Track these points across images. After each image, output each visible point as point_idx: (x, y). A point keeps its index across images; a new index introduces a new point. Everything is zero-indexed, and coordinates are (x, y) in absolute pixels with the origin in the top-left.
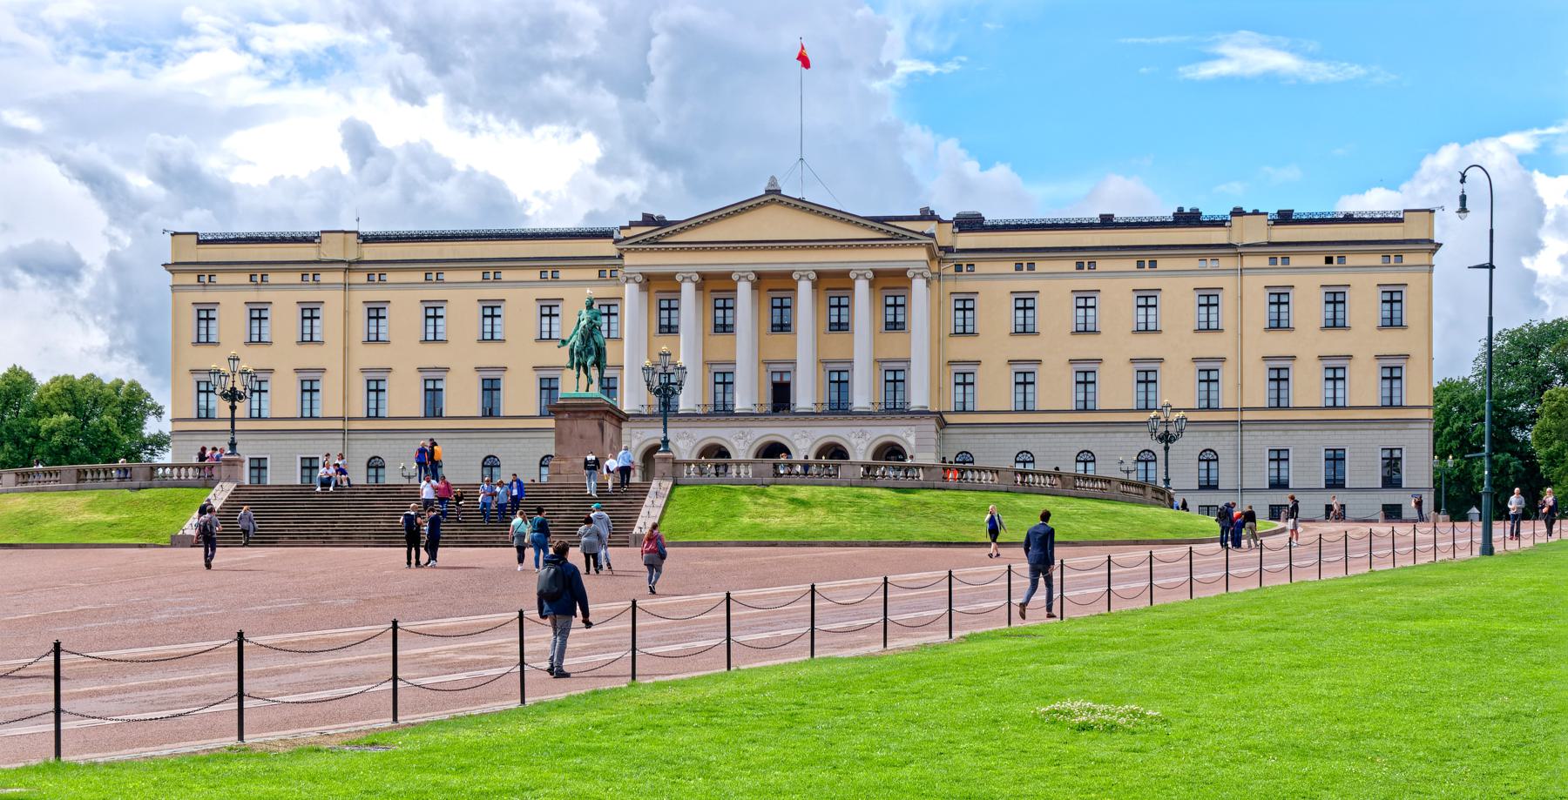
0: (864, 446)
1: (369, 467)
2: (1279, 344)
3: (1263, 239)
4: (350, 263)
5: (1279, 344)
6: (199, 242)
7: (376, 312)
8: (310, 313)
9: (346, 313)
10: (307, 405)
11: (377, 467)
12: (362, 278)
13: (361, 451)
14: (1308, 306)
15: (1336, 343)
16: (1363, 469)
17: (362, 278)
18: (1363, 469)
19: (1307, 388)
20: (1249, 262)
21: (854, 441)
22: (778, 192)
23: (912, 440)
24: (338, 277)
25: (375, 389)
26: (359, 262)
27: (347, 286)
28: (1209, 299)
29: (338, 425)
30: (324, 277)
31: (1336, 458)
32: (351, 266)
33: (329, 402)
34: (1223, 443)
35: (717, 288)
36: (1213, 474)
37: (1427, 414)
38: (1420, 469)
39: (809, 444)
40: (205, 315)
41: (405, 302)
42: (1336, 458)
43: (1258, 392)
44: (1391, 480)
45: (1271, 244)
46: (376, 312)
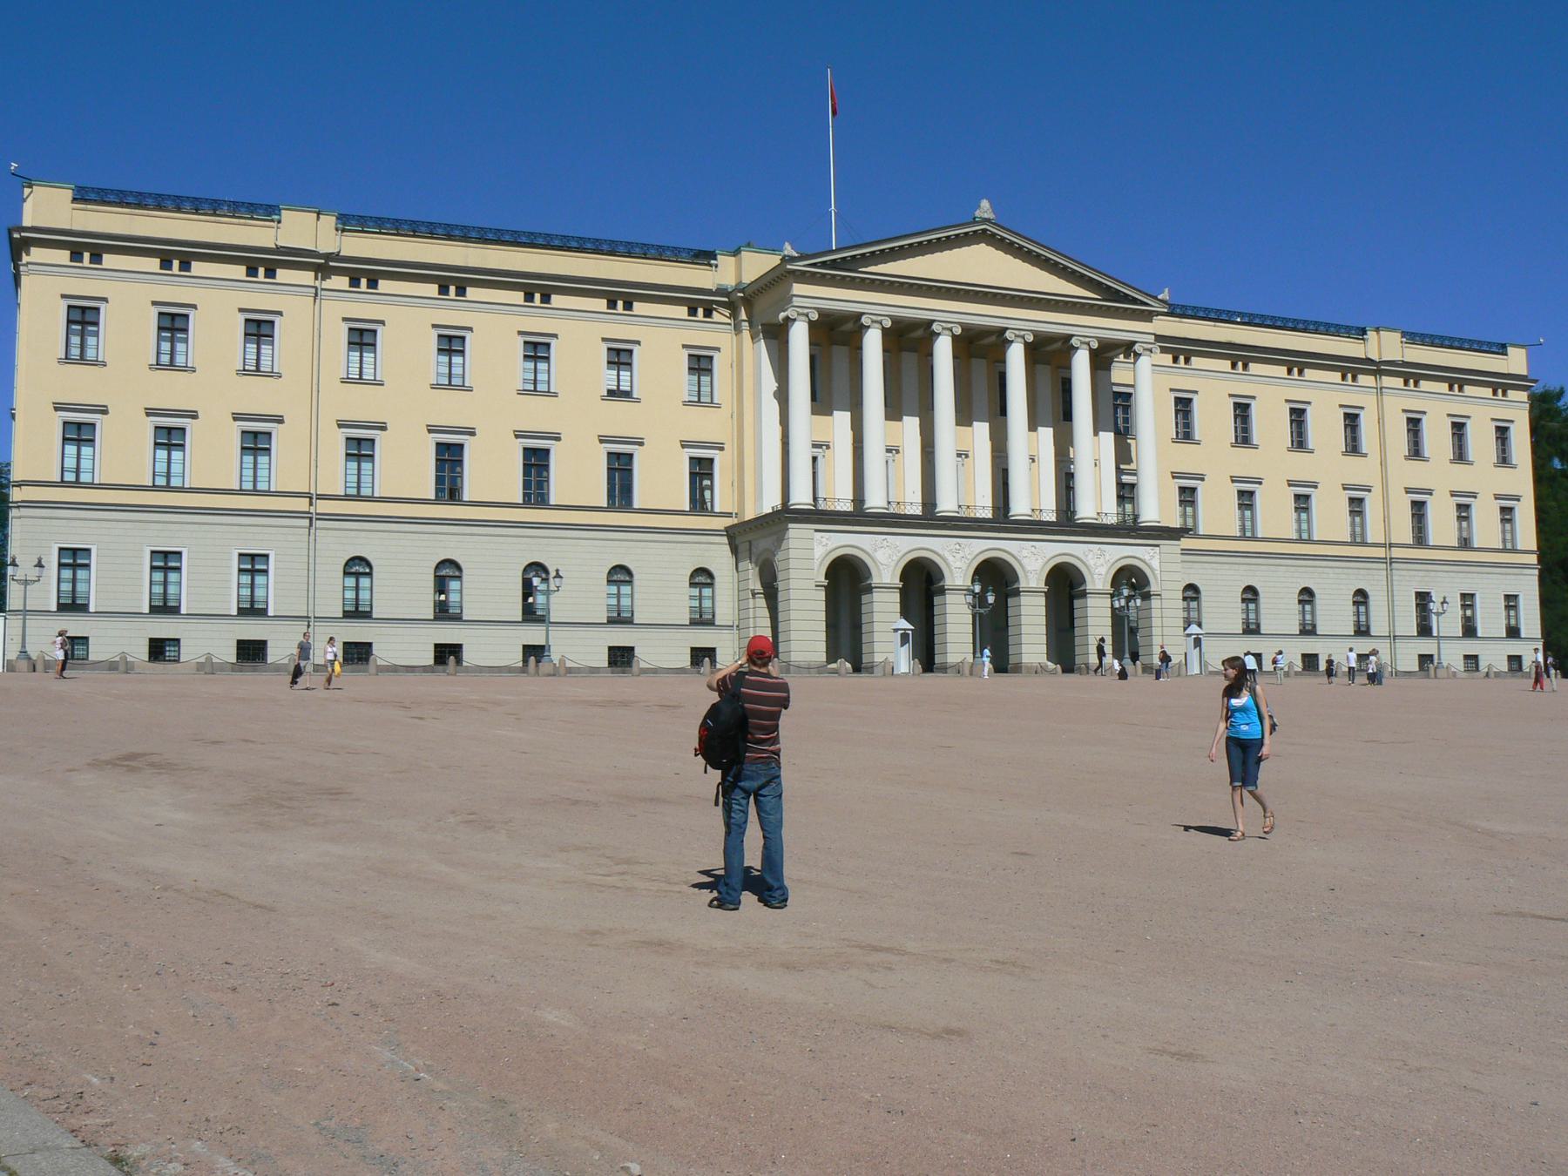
0: (1103, 570)
1: (346, 574)
2: (1417, 474)
3: (1398, 358)
4: (329, 257)
5: (1417, 474)
6: (75, 200)
7: (362, 338)
8: (259, 329)
9: (317, 335)
10: (249, 473)
12: (341, 282)
13: (339, 545)
14: (1437, 437)
15: (1462, 477)
16: (1491, 620)
17: (341, 282)
19: (1441, 525)
20: (1387, 381)
21: (1091, 562)
24: (307, 277)
25: (360, 450)
26: (336, 257)
28: (1352, 420)
29: (302, 505)
30: (283, 275)
32: (324, 265)
33: (287, 466)
34: (1374, 583)
35: (909, 341)
36: (1363, 618)
37: (1533, 559)
39: (1040, 562)
45: (1405, 364)
46: (362, 338)
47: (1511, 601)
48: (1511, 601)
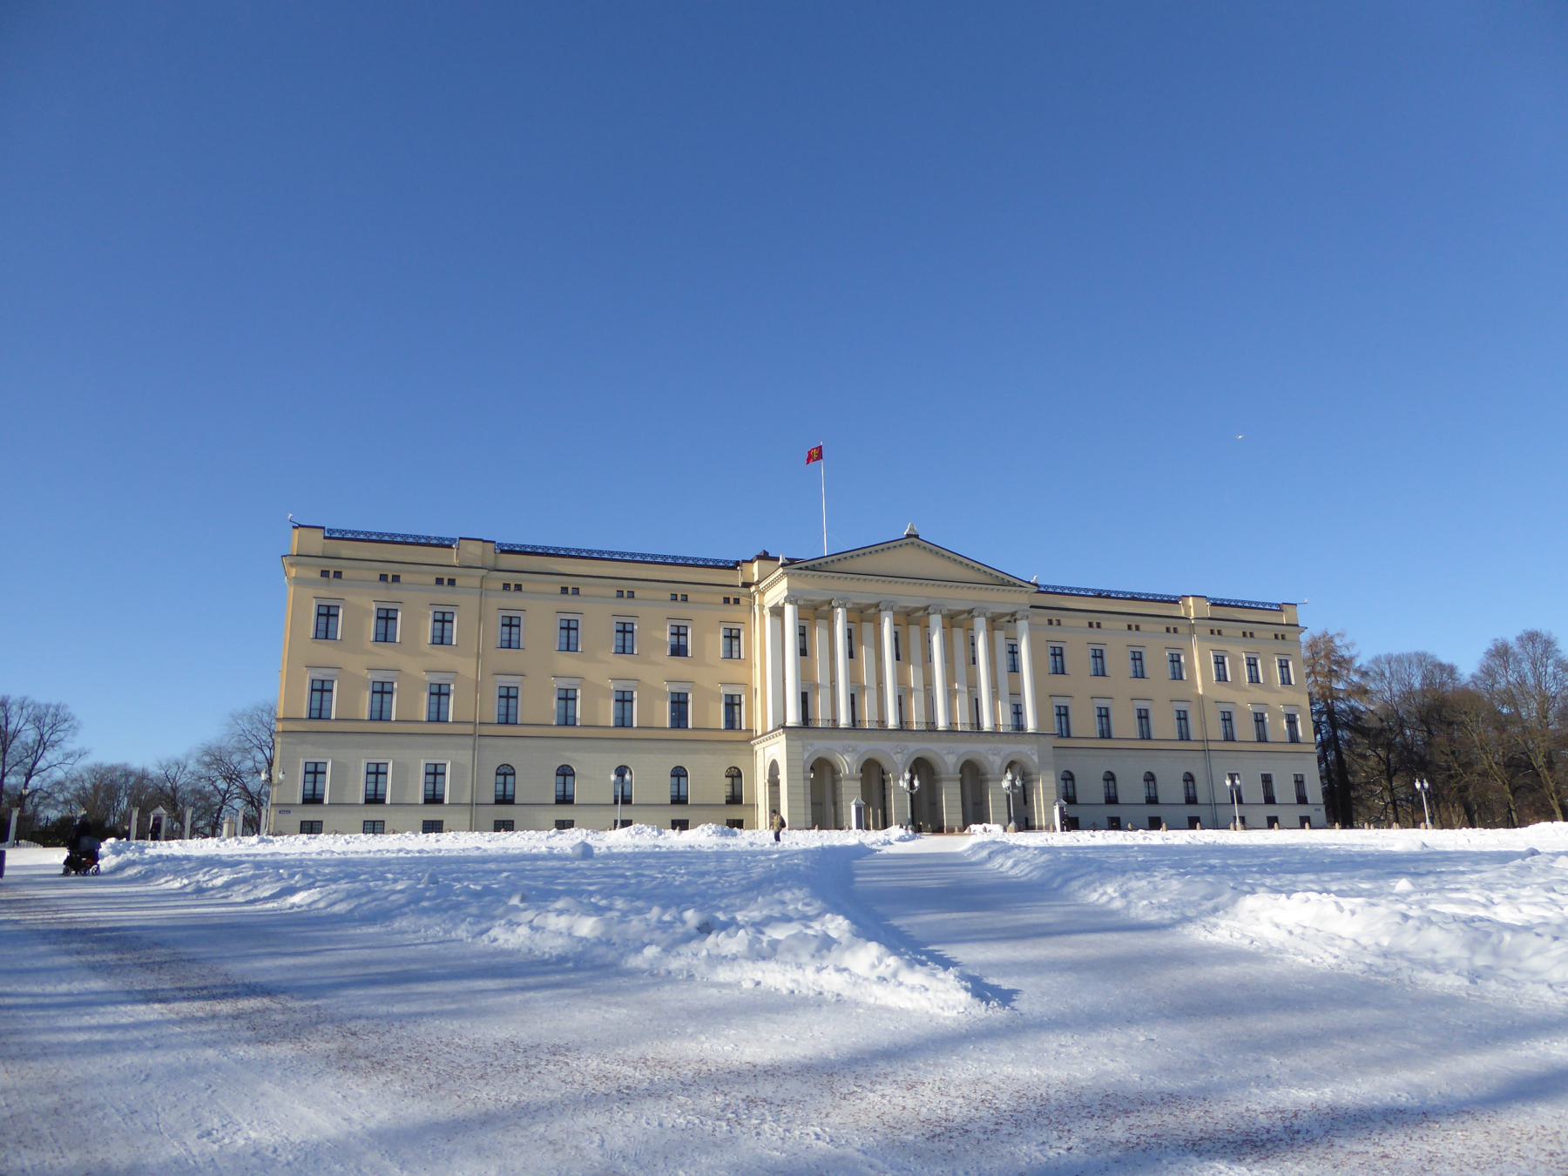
7: (511, 623)
11: (505, 775)
16: (1284, 791)
18: (1284, 791)
22: (917, 536)
23: (1036, 759)
27: (483, 591)
29: (469, 729)
31: (1267, 780)
38: (1315, 790)
40: (327, 614)
41: (541, 616)
42: (1267, 780)
43: (1216, 731)
44: (1302, 800)
46: (511, 623)
47: (1299, 782)
48: (1299, 782)
